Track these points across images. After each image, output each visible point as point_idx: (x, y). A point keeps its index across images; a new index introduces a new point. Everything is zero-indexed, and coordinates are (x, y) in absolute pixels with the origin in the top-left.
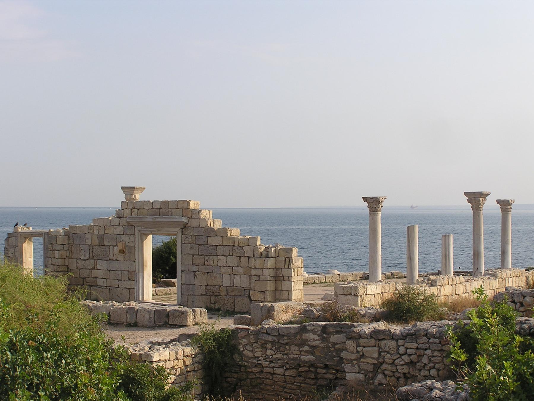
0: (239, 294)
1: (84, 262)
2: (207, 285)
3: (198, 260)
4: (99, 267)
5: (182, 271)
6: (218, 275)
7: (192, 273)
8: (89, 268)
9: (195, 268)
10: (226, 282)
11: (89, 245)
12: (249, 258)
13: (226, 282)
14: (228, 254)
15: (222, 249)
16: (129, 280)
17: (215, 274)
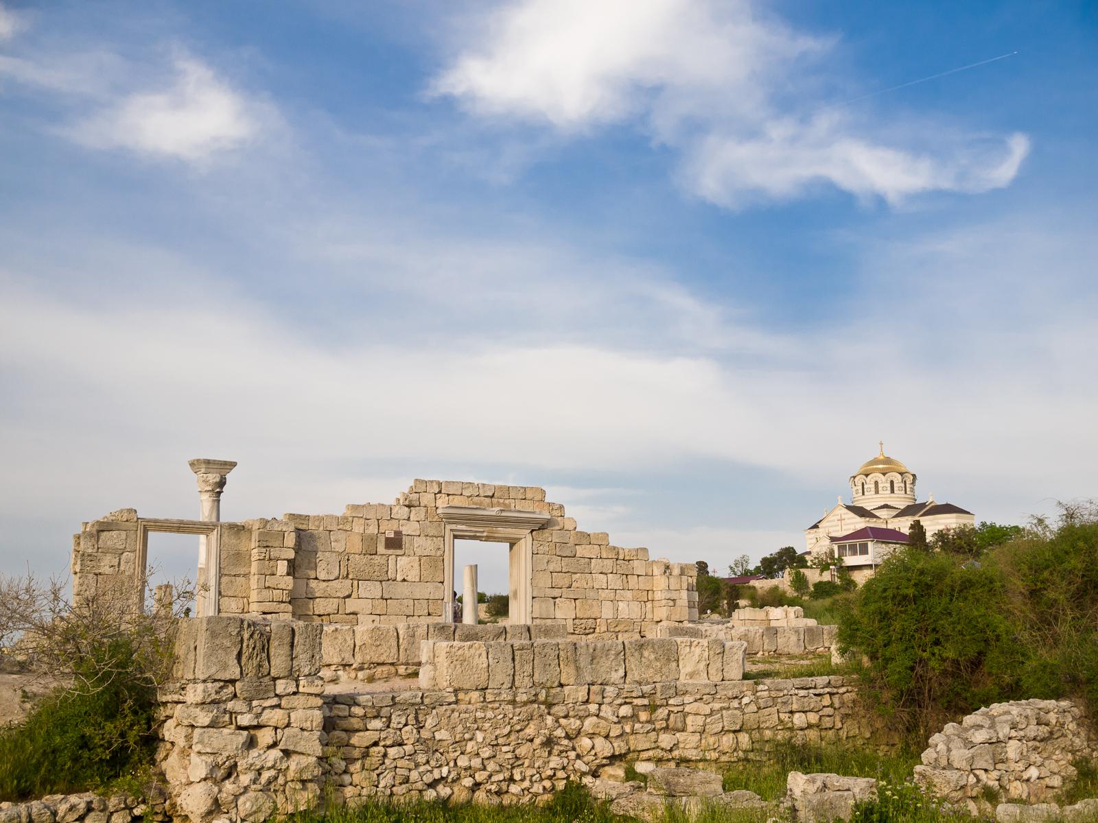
0: (626, 629)
1: (325, 584)
2: (576, 618)
3: (563, 580)
4: (362, 593)
5: (533, 598)
6: (595, 603)
7: (552, 601)
8: (339, 594)
9: (556, 593)
10: (607, 612)
11: (340, 554)
12: (638, 576)
13: (607, 612)
14: (610, 571)
15: (601, 564)
16: (429, 615)
17: (590, 601)
